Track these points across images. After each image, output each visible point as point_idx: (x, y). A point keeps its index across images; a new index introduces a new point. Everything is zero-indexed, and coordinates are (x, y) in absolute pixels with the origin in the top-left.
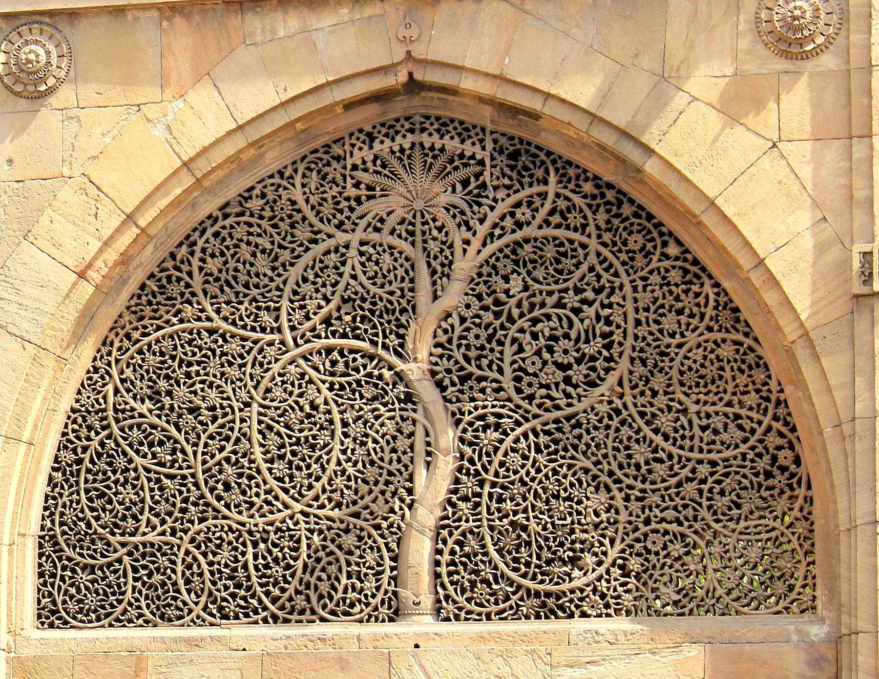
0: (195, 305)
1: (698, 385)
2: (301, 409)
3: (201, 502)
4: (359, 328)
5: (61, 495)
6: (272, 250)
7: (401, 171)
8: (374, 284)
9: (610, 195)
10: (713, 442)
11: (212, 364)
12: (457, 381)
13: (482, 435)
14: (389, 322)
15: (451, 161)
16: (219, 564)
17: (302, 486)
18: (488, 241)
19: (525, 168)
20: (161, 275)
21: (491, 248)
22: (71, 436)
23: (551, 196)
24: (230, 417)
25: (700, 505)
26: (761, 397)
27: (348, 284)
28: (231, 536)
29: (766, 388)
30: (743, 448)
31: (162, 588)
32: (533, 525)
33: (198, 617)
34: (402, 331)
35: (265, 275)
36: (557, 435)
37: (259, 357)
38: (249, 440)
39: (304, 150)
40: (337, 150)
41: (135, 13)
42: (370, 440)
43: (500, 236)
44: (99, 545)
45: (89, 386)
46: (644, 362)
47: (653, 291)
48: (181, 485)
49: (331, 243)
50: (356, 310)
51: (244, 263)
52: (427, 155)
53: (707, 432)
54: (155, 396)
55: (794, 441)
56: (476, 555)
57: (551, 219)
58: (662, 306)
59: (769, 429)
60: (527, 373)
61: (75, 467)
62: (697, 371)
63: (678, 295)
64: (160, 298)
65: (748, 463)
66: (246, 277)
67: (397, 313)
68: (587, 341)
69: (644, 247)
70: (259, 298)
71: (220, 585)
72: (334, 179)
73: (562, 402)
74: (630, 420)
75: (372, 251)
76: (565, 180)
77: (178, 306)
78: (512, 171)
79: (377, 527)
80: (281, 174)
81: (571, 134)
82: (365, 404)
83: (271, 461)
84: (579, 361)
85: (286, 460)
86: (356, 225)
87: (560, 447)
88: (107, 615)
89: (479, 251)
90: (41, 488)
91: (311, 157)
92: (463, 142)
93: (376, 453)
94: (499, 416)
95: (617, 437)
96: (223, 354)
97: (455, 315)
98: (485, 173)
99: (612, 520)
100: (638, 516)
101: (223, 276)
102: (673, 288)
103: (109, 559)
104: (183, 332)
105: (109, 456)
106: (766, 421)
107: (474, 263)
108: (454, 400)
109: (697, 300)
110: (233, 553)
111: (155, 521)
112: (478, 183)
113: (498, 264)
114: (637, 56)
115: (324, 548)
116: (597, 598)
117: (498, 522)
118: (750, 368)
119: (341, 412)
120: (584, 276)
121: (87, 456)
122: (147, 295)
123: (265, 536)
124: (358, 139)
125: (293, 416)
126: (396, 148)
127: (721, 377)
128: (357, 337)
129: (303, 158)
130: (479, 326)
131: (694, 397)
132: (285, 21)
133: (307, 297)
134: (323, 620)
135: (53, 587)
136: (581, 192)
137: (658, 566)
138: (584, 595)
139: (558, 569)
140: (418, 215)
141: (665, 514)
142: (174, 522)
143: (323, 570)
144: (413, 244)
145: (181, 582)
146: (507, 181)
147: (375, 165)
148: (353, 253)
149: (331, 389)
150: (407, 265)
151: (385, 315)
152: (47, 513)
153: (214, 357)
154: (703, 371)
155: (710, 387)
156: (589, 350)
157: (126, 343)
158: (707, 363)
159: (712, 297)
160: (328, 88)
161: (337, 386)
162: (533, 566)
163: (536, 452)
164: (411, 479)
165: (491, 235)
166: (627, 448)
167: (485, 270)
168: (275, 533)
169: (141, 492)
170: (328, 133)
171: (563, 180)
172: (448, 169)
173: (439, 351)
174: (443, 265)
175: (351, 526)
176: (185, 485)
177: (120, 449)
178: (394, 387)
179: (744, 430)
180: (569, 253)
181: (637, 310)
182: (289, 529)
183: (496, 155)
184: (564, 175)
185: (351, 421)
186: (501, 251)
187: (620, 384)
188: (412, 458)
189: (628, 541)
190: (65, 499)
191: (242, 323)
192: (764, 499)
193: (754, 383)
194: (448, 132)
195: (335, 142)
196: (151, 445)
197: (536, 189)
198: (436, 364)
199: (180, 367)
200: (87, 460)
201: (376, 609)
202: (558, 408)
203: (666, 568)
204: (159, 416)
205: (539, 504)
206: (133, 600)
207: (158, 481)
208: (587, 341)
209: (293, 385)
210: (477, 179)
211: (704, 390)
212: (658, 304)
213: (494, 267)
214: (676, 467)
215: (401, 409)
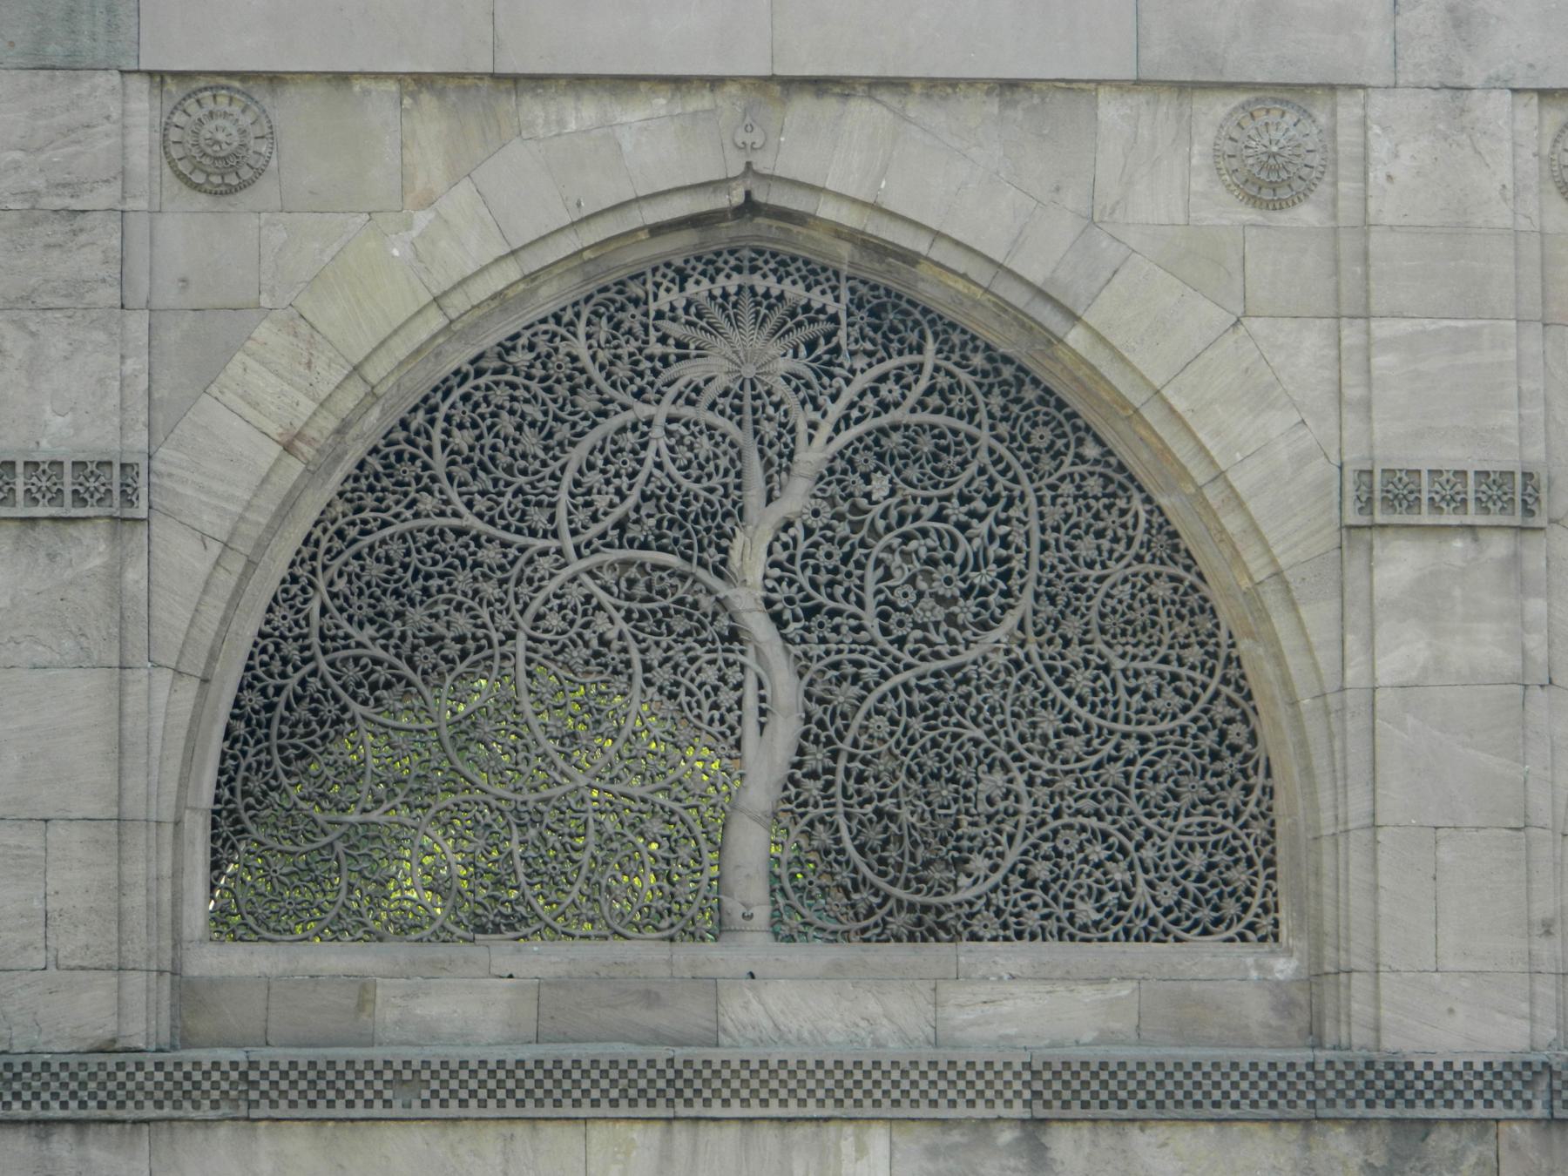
0: (437, 494)
1: (1124, 633)
2: (586, 644)
4: (663, 536)
5: (244, 753)
6: (544, 423)
7: (724, 323)
8: (687, 477)
9: (1007, 372)
10: (1143, 710)
11: (461, 578)
12: (800, 612)
14: (708, 530)
15: (793, 315)
18: (842, 426)
19: (894, 330)
20: (387, 450)
21: (846, 436)
22: (260, 672)
23: (928, 369)
24: (487, 652)
25: (1126, 792)
26: (1207, 653)
27: (651, 475)
29: (1213, 640)
30: (1184, 719)
32: (905, 814)
34: (724, 543)
35: (535, 457)
36: (938, 693)
39: (592, 287)
40: (635, 290)
41: (365, 83)
42: (682, 691)
43: (858, 421)
45: (285, 601)
46: (1052, 600)
47: (1064, 505)
49: (627, 417)
50: (660, 511)
51: (506, 440)
52: (758, 304)
53: (1137, 697)
56: (827, 853)
58: (1076, 526)
59: (1217, 694)
60: (897, 609)
61: (263, 716)
62: (1123, 614)
63: (1098, 511)
64: (386, 482)
65: (1189, 739)
66: (509, 459)
67: (719, 519)
68: (976, 568)
69: (1052, 443)
70: (527, 488)
73: (945, 649)
74: (1034, 676)
75: (683, 431)
76: (946, 348)
77: (412, 495)
80: (557, 319)
82: (675, 641)
84: (966, 594)
86: (663, 394)
87: (941, 708)
89: (830, 440)
90: (216, 744)
91: (599, 298)
92: (808, 288)
93: (691, 710)
94: (859, 664)
96: (476, 564)
97: (798, 524)
99: (1011, 810)
100: (1045, 806)
101: (476, 456)
102: (1092, 502)
104: (420, 530)
105: (313, 700)
107: (822, 455)
109: (1123, 520)
113: (857, 458)
114: (1058, 189)
117: (857, 810)
118: (1192, 613)
119: (643, 651)
121: (281, 700)
122: (367, 478)
124: (664, 276)
125: (575, 654)
126: (717, 292)
127: (1154, 624)
128: (662, 549)
129: (588, 299)
130: (830, 540)
131: (1120, 650)
132: (576, 109)
137: (1073, 873)
138: (975, 909)
139: (937, 874)
140: (748, 386)
141: (1080, 804)
144: (740, 424)
147: (686, 311)
148: (657, 431)
149: (627, 619)
150: (733, 453)
151: (702, 520)
152: (224, 779)
153: (464, 567)
154: (1130, 615)
155: (1140, 636)
156: (980, 579)
157: (338, 544)
158: (1137, 605)
159: (1143, 516)
160: (635, 206)
161: (636, 615)
165: (846, 418)
167: (839, 464)
170: (626, 266)
171: (945, 348)
172: (790, 324)
173: (777, 572)
174: (780, 455)
180: (953, 448)
181: (1043, 529)
183: (853, 308)
184: (945, 342)
185: (656, 663)
186: (860, 439)
187: (1021, 627)
189: (1032, 839)
190: (250, 759)
191: (503, 522)
192: (1211, 790)
193: (1197, 633)
194: (788, 274)
195: (632, 278)
196: (374, 687)
197: (907, 359)
198: (773, 590)
199: (415, 578)
200: (281, 706)
202: (938, 656)
204: (385, 648)
209: (575, 611)
210: (828, 341)
211: (1133, 641)
213: (851, 461)
214: (1096, 742)
215: (725, 650)
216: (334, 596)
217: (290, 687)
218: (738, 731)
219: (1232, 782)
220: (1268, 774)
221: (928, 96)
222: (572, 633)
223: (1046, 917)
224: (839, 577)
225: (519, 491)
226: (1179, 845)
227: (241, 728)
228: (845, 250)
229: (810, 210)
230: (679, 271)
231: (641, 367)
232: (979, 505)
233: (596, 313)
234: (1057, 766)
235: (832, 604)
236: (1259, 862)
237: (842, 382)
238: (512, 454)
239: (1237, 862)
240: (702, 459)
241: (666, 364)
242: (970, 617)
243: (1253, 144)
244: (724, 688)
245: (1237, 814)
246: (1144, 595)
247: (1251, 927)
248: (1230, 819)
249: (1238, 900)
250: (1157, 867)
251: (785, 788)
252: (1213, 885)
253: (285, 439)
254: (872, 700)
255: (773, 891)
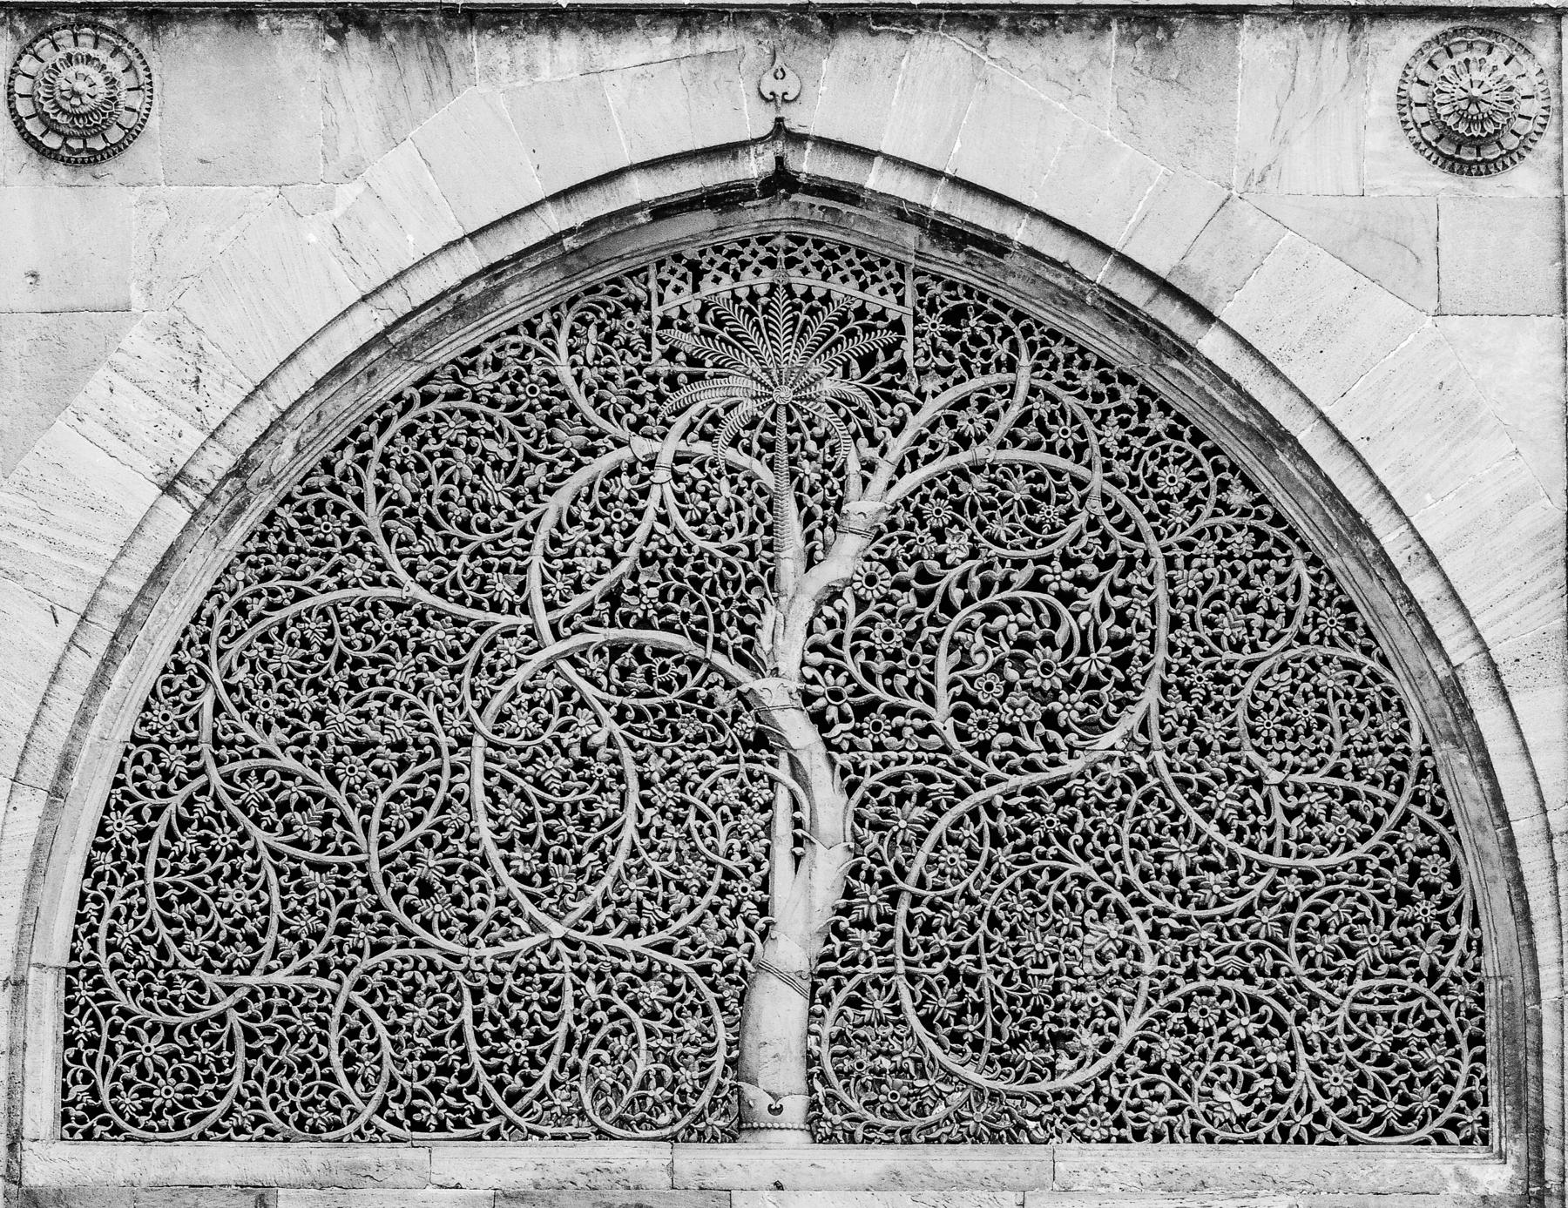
0: (369, 556)
1: (1281, 736)
2: (565, 753)
3: (377, 915)
4: (670, 611)
5: (110, 894)
6: (512, 464)
8: (701, 533)
9: (1127, 395)
10: (1308, 839)
12: (848, 708)
13: (897, 812)
14: (727, 602)
15: (843, 321)
16: (410, 1029)
17: (565, 891)
18: (908, 466)
19: (976, 340)
20: (305, 498)
21: (911, 480)
23: (1022, 390)
24: (433, 763)
25: (1285, 947)
26: (1393, 762)
27: (653, 531)
28: (433, 980)
29: (1401, 746)
30: (1361, 850)
31: (302, 1070)
33: (369, 1126)
35: (500, 508)
36: (1031, 816)
37: (488, 656)
38: (468, 805)
40: (635, 290)
42: (692, 812)
43: (929, 459)
44: (185, 990)
46: (1186, 694)
47: (1202, 568)
48: (339, 883)
49: (624, 454)
50: (665, 579)
51: (461, 485)
52: (799, 307)
53: (1298, 820)
54: (290, 720)
55: (1450, 840)
57: (1021, 432)
59: (1406, 817)
61: (136, 846)
62: (1281, 712)
63: (1247, 576)
64: (301, 540)
65: (1368, 877)
66: (465, 511)
67: (742, 587)
68: (1084, 651)
69: (1187, 487)
70: (488, 548)
71: (411, 1068)
72: (628, 340)
73: (1041, 758)
74: (1161, 794)
75: (696, 473)
76: (1046, 364)
77: (336, 558)
78: (952, 343)
79: (704, 970)
80: (531, 327)
81: (1062, 282)
82: (684, 748)
83: (509, 846)
85: (537, 844)
86: (669, 425)
87: (1036, 837)
88: (196, 1119)
89: (891, 484)
92: (863, 287)
93: (703, 838)
94: (927, 778)
95: (1138, 823)
96: (420, 648)
97: (848, 594)
98: (903, 345)
99: (1128, 970)
100: (1174, 965)
102: (1240, 565)
103: (202, 1015)
105: (202, 825)
106: (1402, 803)
107: (880, 505)
108: (846, 745)
109: (1280, 588)
110: (435, 1009)
111: (291, 948)
112: (892, 361)
115: (606, 1004)
116: (1102, 1108)
117: (923, 969)
118: (1373, 709)
119: (639, 762)
120: (1081, 535)
121: (161, 825)
122: (277, 535)
123: (496, 980)
124: (673, 272)
125: (549, 765)
126: (743, 293)
127: (1322, 724)
129: (571, 302)
130: (891, 615)
133: (578, 552)
134: (600, 1133)
135: (92, 1065)
136: (1074, 388)
137: (1211, 1054)
138: (1080, 1100)
139: (1029, 1054)
142: (326, 951)
143: (603, 1045)
144: (771, 464)
145: (337, 1061)
146: (942, 361)
147: (702, 320)
148: (662, 475)
149: (620, 719)
150: (761, 502)
151: (720, 591)
152: (83, 928)
153: (404, 653)
154: (1291, 713)
155: (1302, 740)
156: (1089, 666)
157: (237, 622)
158: (1298, 700)
159: (1307, 583)
161: (631, 715)
162: (987, 1047)
163: (994, 845)
164: (765, 886)
165: (913, 456)
166: (1155, 843)
167: (902, 517)
168: (516, 976)
169: (263, 894)
170: (621, 258)
173: (818, 658)
174: (825, 505)
175: (657, 967)
176: (346, 884)
177: (224, 814)
178: (735, 719)
179: (1362, 820)
180: (1054, 494)
181: (1174, 600)
182: (541, 969)
183: (923, 313)
184: (1044, 356)
185: (656, 777)
186: (931, 484)
187: (1144, 728)
188: (768, 847)
190: (117, 902)
192: (1399, 943)
193: (1378, 735)
194: (837, 268)
195: (630, 275)
197: (994, 378)
198: (814, 681)
199: (339, 667)
200: (159, 838)
201: (700, 1117)
202: (1032, 767)
203: (1225, 1057)
204: (298, 757)
205: (999, 938)
206: (245, 1093)
207: (296, 874)
208: (1084, 651)
209: (549, 707)
210: (888, 356)
212: (1211, 590)
213: (918, 513)
214: (1242, 880)
215: (747, 760)
216: (231, 689)
217: (172, 808)
218: (765, 866)
219: (1427, 933)
220: (1476, 923)
221: (1018, 32)
222: (546, 738)
223: (1173, 1111)
224: (901, 664)
225: (479, 552)
226: (1355, 1016)
227: (106, 861)
228: (910, 236)
229: (858, 181)
230: (693, 266)
231: (641, 391)
232: (1090, 570)
233: (582, 321)
234: (1191, 911)
235: (892, 699)
236: (1462, 1040)
237: (907, 409)
238: (469, 502)
239: (1432, 1039)
240: (720, 509)
241: (674, 387)
242: (1074, 714)
243: (1448, 87)
244: (748, 810)
245: (1434, 975)
246: (1308, 687)
247: (1452, 1124)
248: (1424, 982)
249: (1435, 1089)
250: (1324, 1045)
251: (828, 941)
252: (1401, 1069)
253: (163, 480)
254: (944, 823)
255: (810, 1076)
